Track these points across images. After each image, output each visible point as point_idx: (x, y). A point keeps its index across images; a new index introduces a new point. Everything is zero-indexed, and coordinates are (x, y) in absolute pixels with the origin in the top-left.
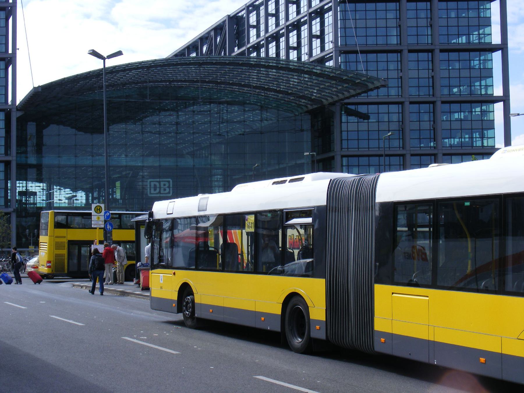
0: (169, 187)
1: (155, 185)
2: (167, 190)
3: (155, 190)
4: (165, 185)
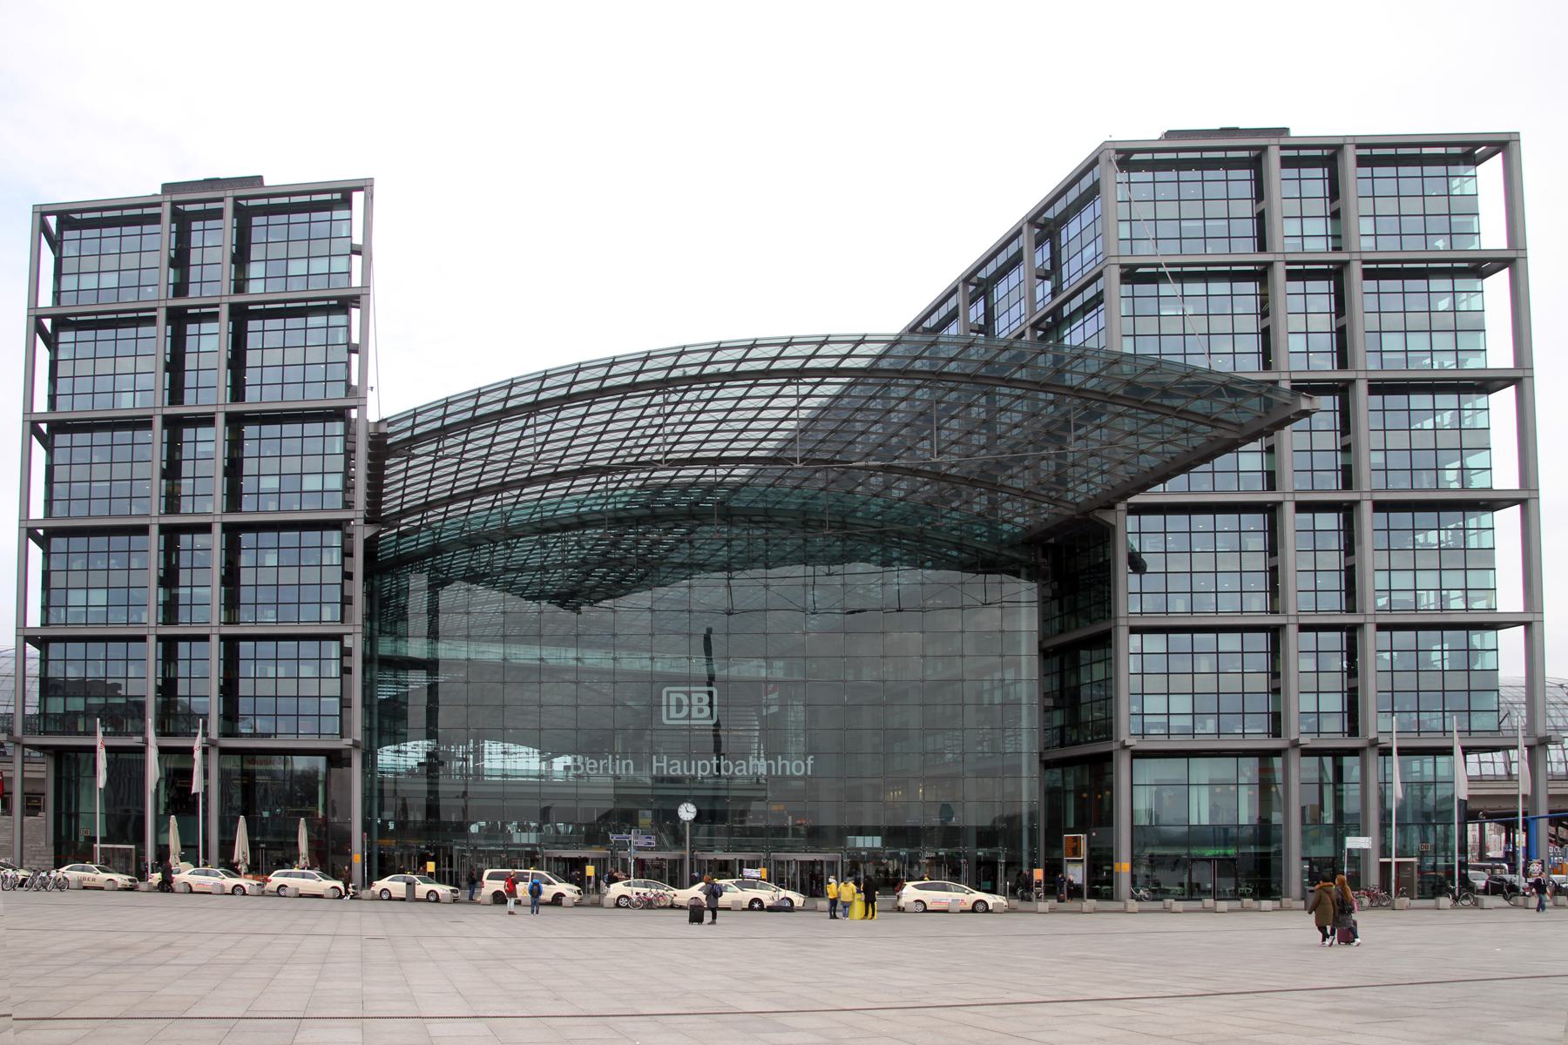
1: (679, 701)
2: (707, 710)
4: (700, 700)
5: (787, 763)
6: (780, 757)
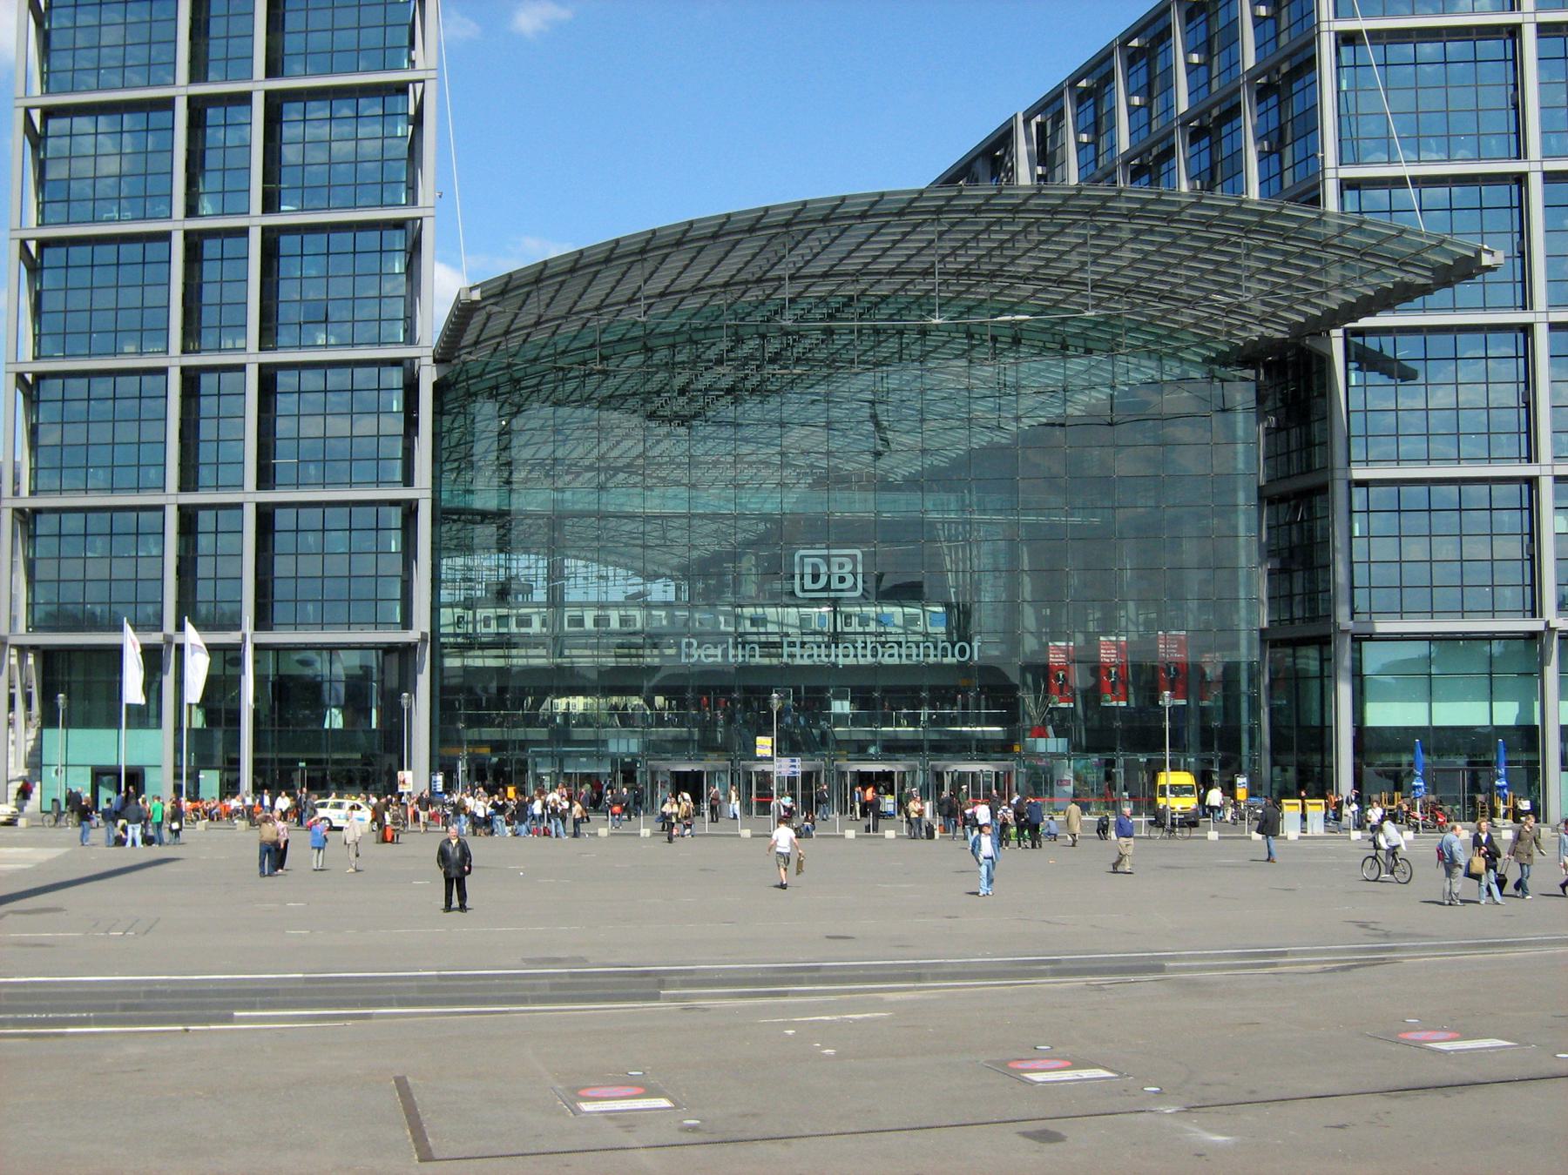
1: (815, 566)
4: (841, 566)
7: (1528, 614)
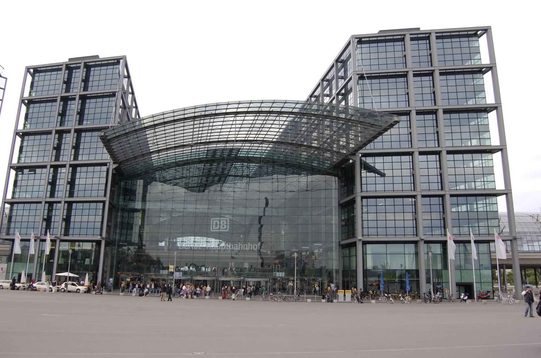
0: (227, 225)
1: (216, 223)
2: (225, 226)
3: (216, 227)
4: (223, 223)
5: (251, 245)
6: (249, 243)
7: (415, 236)
